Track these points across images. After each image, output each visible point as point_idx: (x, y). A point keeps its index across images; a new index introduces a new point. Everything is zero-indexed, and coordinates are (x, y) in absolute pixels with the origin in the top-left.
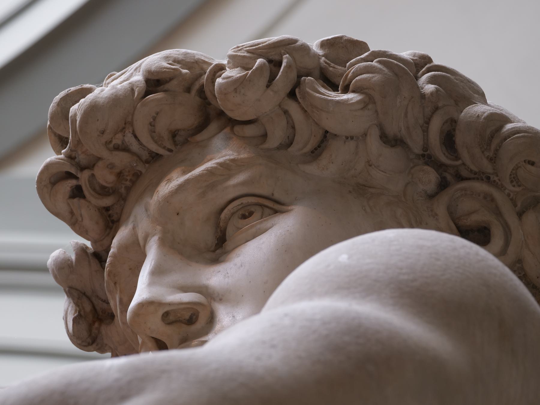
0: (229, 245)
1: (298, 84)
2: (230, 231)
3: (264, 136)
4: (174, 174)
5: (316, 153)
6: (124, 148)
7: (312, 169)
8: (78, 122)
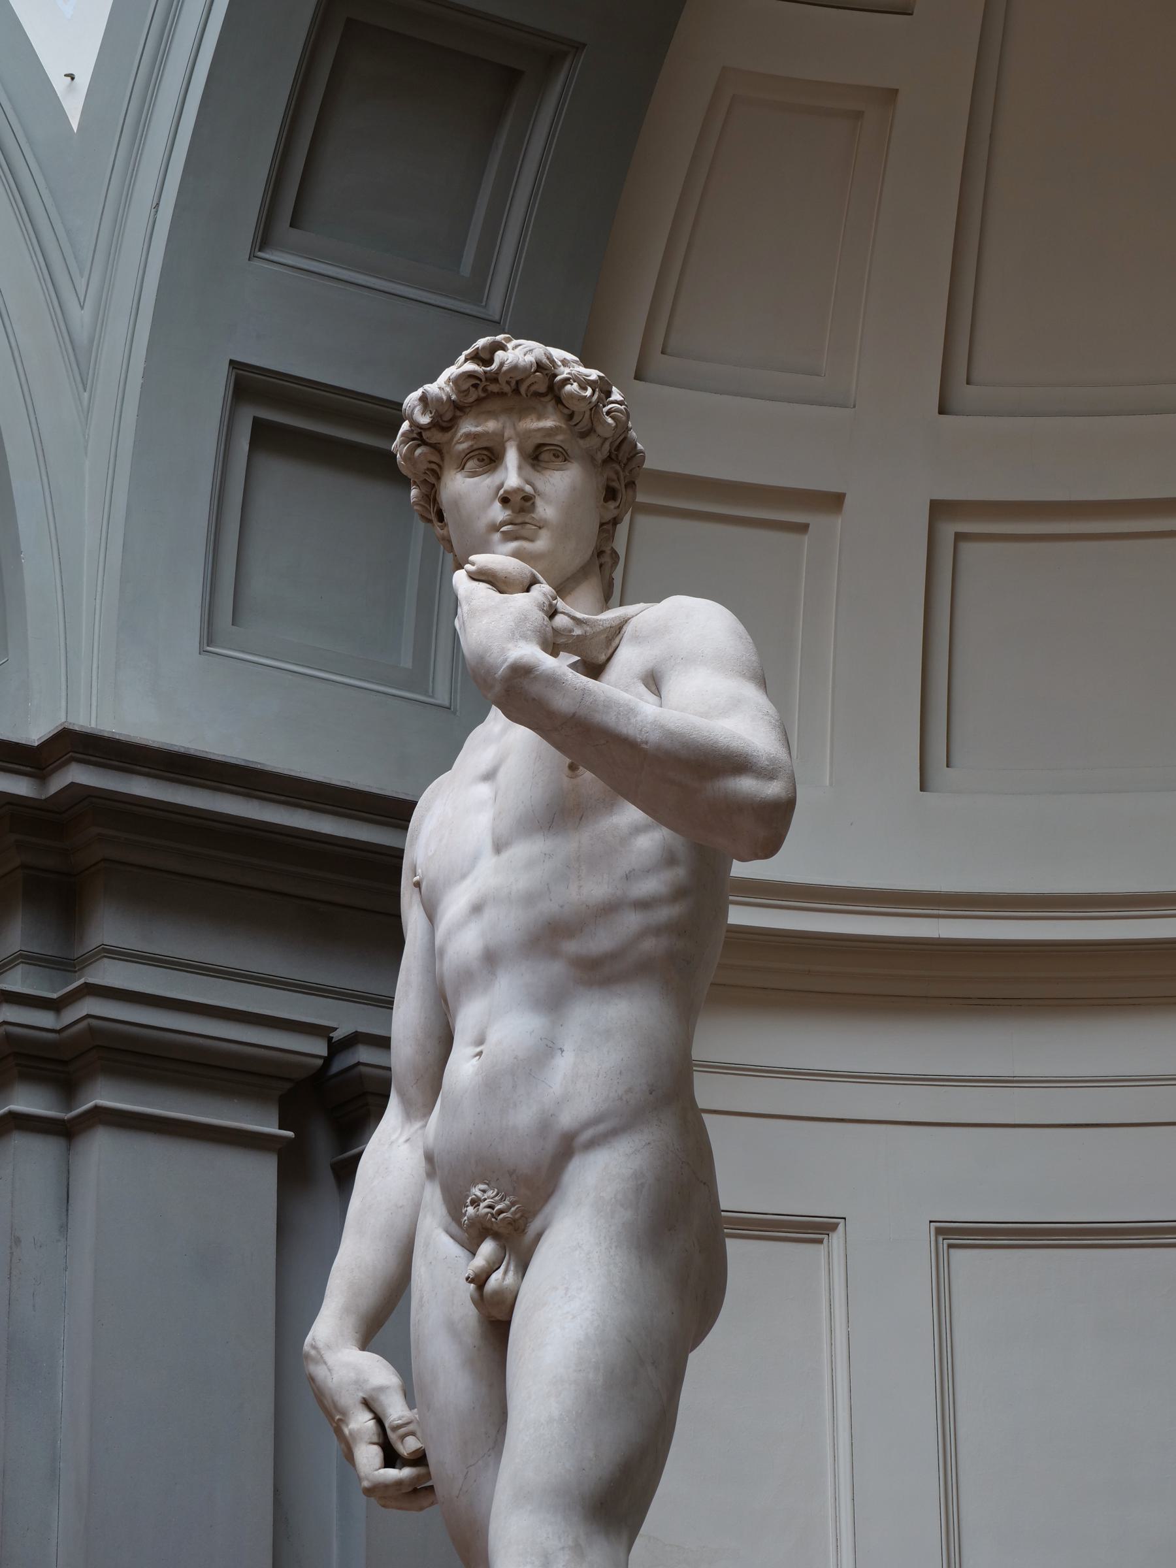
0: (543, 464)
1: (596, 405)
2: (545, 456)
3: (571, 416)
4: (534, 416)
5: (584, 435)
6: (508, 383)
7: (581, 442)
8: (504, 369)
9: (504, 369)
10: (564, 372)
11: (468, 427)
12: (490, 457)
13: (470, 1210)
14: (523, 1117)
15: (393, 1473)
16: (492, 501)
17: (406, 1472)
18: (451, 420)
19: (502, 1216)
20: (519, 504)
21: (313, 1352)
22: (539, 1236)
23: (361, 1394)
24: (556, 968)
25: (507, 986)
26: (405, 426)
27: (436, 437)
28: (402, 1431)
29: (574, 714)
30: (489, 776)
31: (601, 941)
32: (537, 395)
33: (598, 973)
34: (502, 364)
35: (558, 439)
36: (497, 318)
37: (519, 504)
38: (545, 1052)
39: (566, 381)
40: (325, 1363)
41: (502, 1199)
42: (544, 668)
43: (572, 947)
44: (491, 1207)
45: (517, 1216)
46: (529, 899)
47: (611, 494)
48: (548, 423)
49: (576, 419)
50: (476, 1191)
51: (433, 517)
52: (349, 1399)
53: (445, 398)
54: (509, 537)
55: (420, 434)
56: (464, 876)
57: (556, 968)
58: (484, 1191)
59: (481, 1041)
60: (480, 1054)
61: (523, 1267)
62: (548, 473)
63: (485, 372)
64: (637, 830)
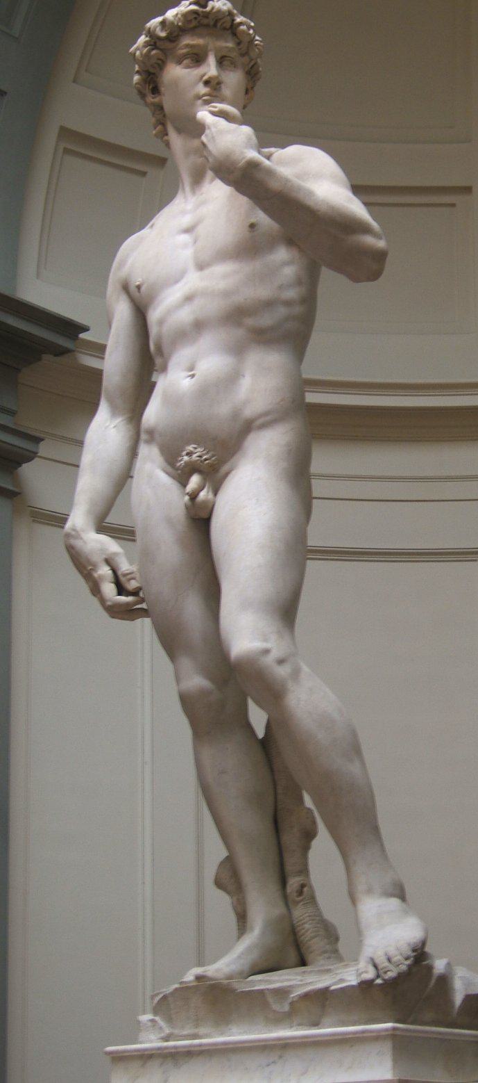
2: (225, 63)
5: (243, 55)
6: (213, 20)
9: (214, 10)
10: (239, 19)
11: (187, 41)
12: (197, 58)
13: (186, 458)
14: (223, 409)
15: (123, 599)
16: (199, 82)
17: (130, 599)
18: (175, 37)
19: (207, 462)
20: (213, 85)
21: (73, 533)
22: (227, 474)
23: (104, 556)
24: (239, 333)
25: (207, 340)
26: (143, 39)
27: (168, 45)
28: (129, 577)
29: (281, 191)
30: (188, 230)
31: (266, 320)
32: (225, 29)
33: (263, 337)
34: (213, 8)
35: (233, 55)
36: (17, 36)
37: (213, 85)
38: (232, 378)
39: (241, 24)
40: (81, 539)
41: (206, 454)
42: (264, 164)
43: (250, 322)
44: (200, 456)
45: (216, 462)
46: (226, 294)
47: (247, 92)
48: (230, 45)
49: (242, 46)
50: (190, 448)
51: (147, 91)
52: (97, 558)
53: (176, 24)
54: (207, 103)
55: (155, 43)
56: (176, 282)
57: (239, 333)
58: (195, 448)
59: (191, 369)
60: (193, 376)
61: (216, 493)
62: (227, 72)
63: (203, 12)
64: (285, 264)
